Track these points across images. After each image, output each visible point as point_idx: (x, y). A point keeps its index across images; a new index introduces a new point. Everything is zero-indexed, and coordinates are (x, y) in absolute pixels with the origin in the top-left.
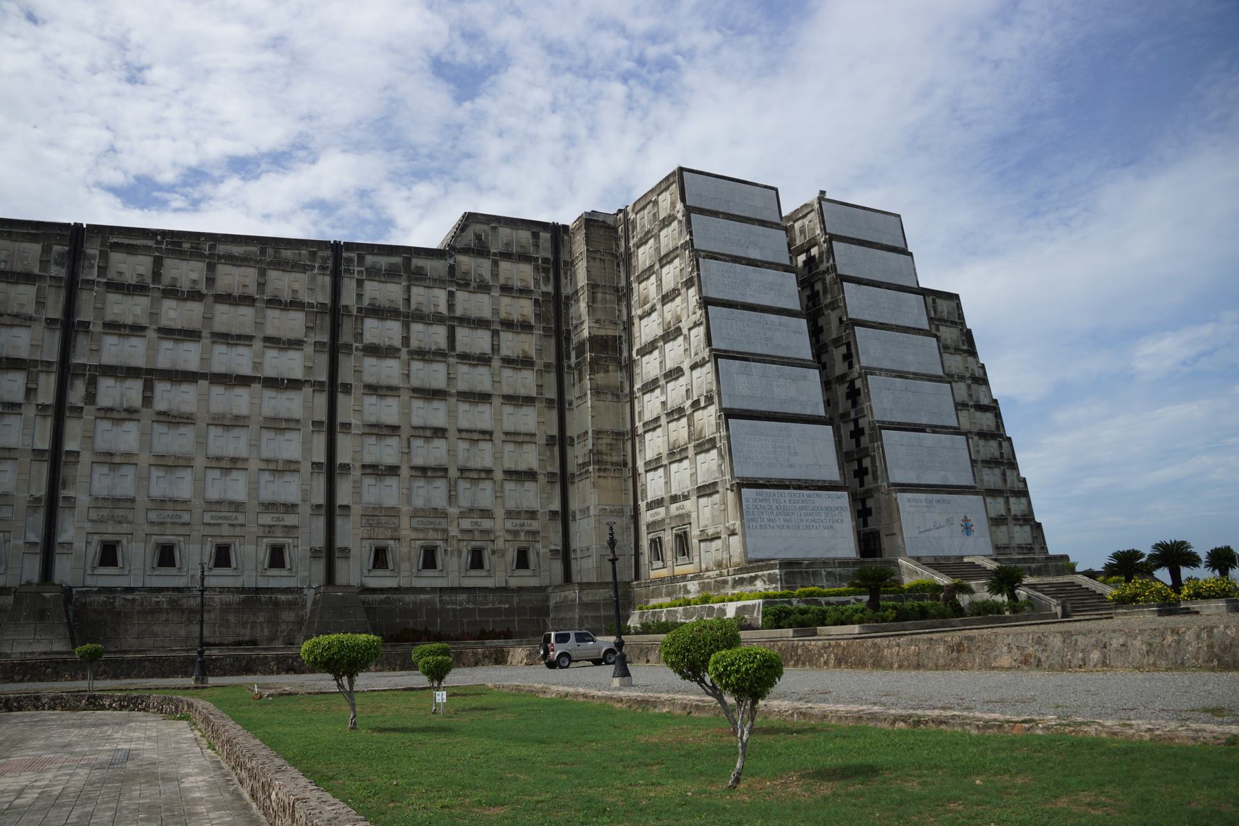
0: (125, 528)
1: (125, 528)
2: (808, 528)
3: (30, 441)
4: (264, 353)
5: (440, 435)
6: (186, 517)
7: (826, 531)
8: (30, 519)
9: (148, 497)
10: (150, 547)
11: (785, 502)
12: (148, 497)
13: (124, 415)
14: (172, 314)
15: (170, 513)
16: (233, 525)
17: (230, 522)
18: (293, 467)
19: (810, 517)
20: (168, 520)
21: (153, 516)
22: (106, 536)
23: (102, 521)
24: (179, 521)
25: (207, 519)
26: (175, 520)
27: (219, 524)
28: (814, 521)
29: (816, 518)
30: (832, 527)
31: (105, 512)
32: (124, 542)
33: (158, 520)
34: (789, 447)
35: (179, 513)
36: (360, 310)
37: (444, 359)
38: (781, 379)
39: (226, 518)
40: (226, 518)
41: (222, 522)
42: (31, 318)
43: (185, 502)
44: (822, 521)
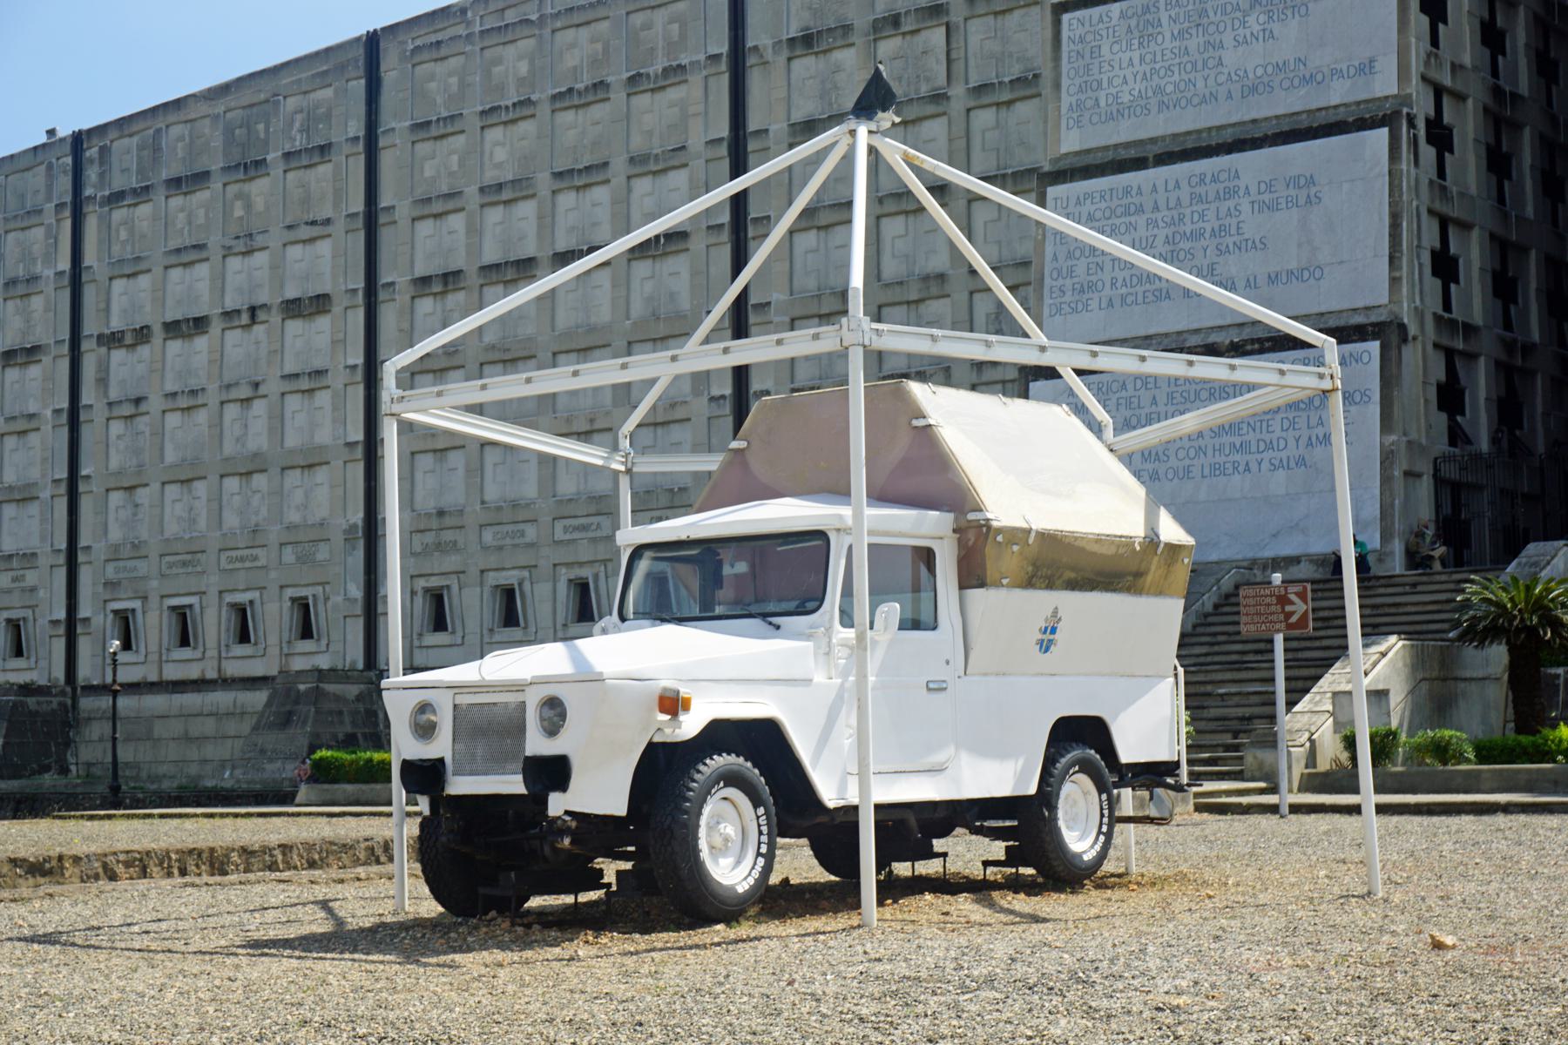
0: (451, 562)
1: (451, 562)
2: (1218, 470)
3: (341, 431)
4: (629, 190)
5: (934, 291)
6: (531, 532)
7: (1281, 473)
8: (350, 560)
9: (483, 502)
10: (487, 590)
11: (1154, 402)
12: (483, 502)
13: (444, 363)
14: (501, 154)
15: (510, 528)
16: (594, 540)
17: (591, 535)
18: (679, 413)
19: (1227, 439)
20: (508, 541)
21: (488, 536)
22: (433, 578)
23: (426, 552)
24: (521, 541)
25: (559, 535)
26: (517, 541)
27: (574, 540)
28: (1243, 448)
29: (1251, 437)
30: (1301, 462)
31: (429, 538)
32: (455, 588)
33: (495, 543)
34: (1223, 230)
35: (521, 526)
36: (777, 44)
37: (940, 109)
38: (1251, 20)
39: (584, 528)
40: (584, 528)
41: (576, 535)
42: (328, 222)
43: (528, 505)
44: (1270, 446)
